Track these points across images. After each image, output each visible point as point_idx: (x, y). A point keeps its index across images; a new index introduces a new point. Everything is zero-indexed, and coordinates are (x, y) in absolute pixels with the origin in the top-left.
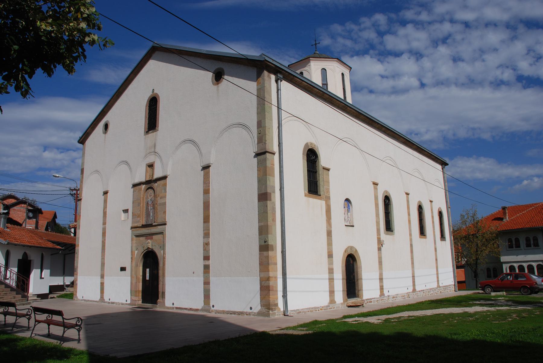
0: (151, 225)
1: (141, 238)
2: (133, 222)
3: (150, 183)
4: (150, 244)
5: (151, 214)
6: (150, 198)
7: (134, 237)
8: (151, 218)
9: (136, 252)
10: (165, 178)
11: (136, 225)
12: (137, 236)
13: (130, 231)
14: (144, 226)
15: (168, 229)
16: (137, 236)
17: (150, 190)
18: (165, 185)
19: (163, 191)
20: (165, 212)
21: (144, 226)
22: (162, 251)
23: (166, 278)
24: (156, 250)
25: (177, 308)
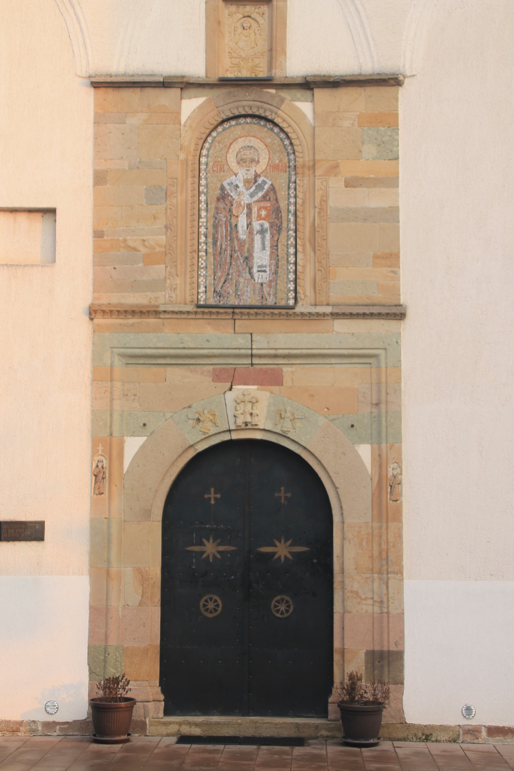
0: (283, 312)
1: (175, 375)
2: (98, 286)
3: (249, 95)
4: (253, 411)
5: (261, 257)
6: (242, 174)
7: (118, 362)
8: (260, 278)
9: (133, 445)
10: (390, 81)
11: (115, 299)
12: (135, 358)
13: (82, 330)
14: (204, 310)
15: (415, 344)
16: (135, 358)
17: (236, 129)
18: (390, 121)
19: (369, 150)
20: (390, 258)
21: (204, 310)
22: (365, 452)
23: (409, 585)
24: (310, 437)
25: (494, 731)
